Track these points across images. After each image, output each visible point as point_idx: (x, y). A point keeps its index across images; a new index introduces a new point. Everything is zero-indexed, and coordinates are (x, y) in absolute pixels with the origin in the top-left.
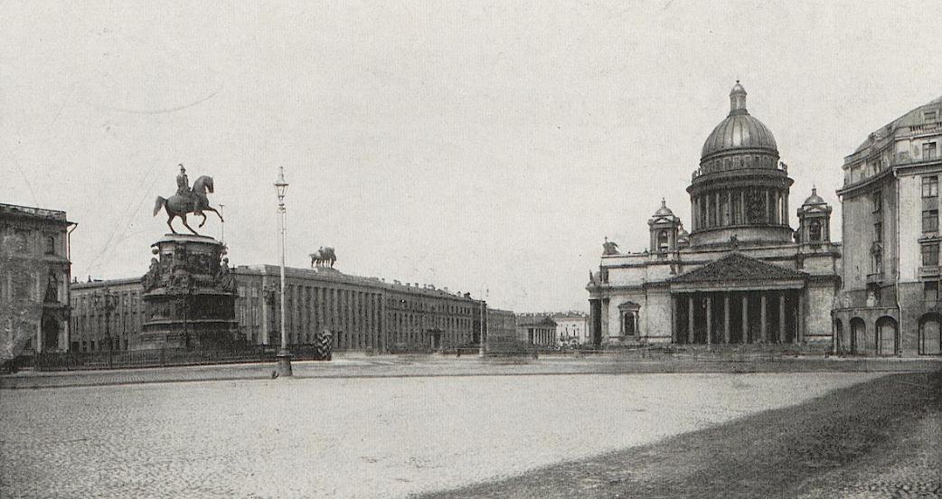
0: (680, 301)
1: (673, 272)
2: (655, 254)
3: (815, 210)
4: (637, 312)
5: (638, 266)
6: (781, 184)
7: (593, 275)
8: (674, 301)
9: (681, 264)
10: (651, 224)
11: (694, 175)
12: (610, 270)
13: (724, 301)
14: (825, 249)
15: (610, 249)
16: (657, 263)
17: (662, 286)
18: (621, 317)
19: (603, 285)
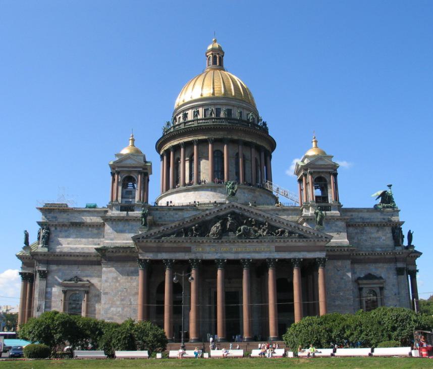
0: (153, 270)
3: (320, 163)
4: (87, 292)
10: (113, 167)
12: (53, 229)
14: (336, 213)
19: (41, 249)
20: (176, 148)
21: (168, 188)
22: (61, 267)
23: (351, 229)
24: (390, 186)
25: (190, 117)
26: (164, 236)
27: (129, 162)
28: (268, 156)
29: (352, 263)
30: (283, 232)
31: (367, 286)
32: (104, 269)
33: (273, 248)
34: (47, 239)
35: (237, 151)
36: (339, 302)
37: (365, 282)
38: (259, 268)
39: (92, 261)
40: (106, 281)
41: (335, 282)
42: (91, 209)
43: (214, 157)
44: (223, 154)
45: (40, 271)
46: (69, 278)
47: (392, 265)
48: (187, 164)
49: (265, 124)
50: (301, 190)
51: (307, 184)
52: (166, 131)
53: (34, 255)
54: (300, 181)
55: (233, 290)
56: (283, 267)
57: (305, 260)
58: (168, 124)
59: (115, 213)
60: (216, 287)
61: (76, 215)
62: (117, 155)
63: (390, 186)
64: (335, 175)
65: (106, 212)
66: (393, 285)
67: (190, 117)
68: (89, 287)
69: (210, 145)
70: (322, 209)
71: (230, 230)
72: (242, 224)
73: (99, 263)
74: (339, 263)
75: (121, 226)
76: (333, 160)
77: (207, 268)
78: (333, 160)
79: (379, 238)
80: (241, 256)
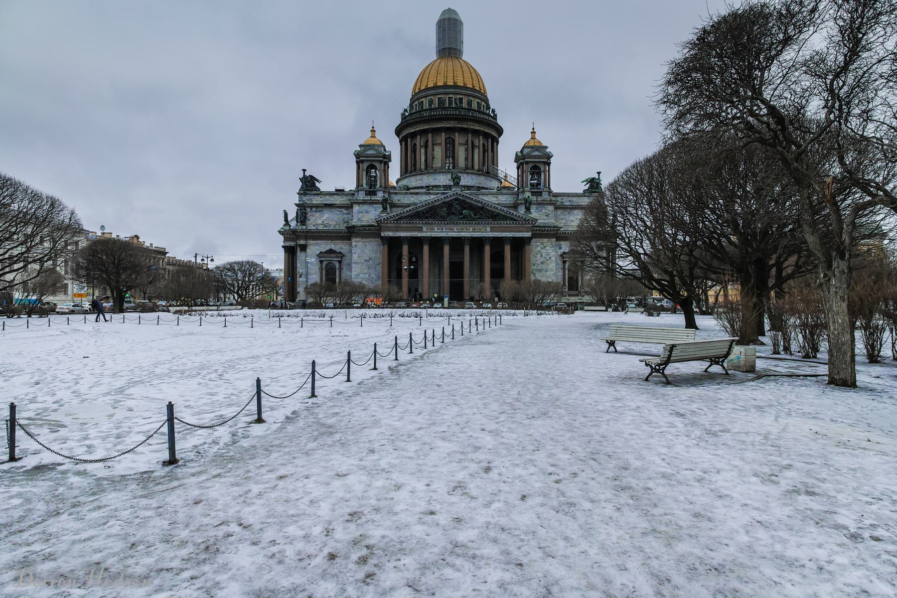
0: (393, 245)
1: (385, 209)
2: (361, 190)
3: (536, 153)
4: (340, 262)
5: (340, 207)
6: (490, 131)
7: (289, 219)
8: (386, 247)
9: (393, 206)
10: (357, 155)
11: (403, 115)
13: (442, 250)
15: (309, 184)
16: (364, 202)
17: (370, 232)
18: (321, 269)
20: (413, 135)
21: (406, 173)
23: (559, 212)
24: (599, 173)
25: (426, 106)
26: (401, 218)
27: (371, 152)
28: (495, 141)
29: (557, 240)
30: (497, 215)
32: (354, 244)
33: (488, 229)
34: (302, 217)
38: (477, 244)
42: (340, 192)
43: (446, 144)
44: (454, 141)
48: (423, 150)
49: (493, 111)
50: (518, 176)
51: (523, 172)
52: (404, 117)
53: (294, 232)
54: (518, 168)
55: (458, 260)
56: (497, 243)
57: (514, 238)
58: (406, 110)
59: (361, 196)
60: (443, 258)
61: (328, 197)
62: (360, 146)
63: (599, 173)
64: (549, 164)
65: (353, 194)
67: (426, 106)
69: (443, 134)
70: (533, 193)
71: (454, 214)
72: (465, 209)
73: (349, 238)
74: (545, 240)
75: (365, 207)
76: (548, 150)
77: (436, 244)
78: (548, 150)
80: (463, 234)
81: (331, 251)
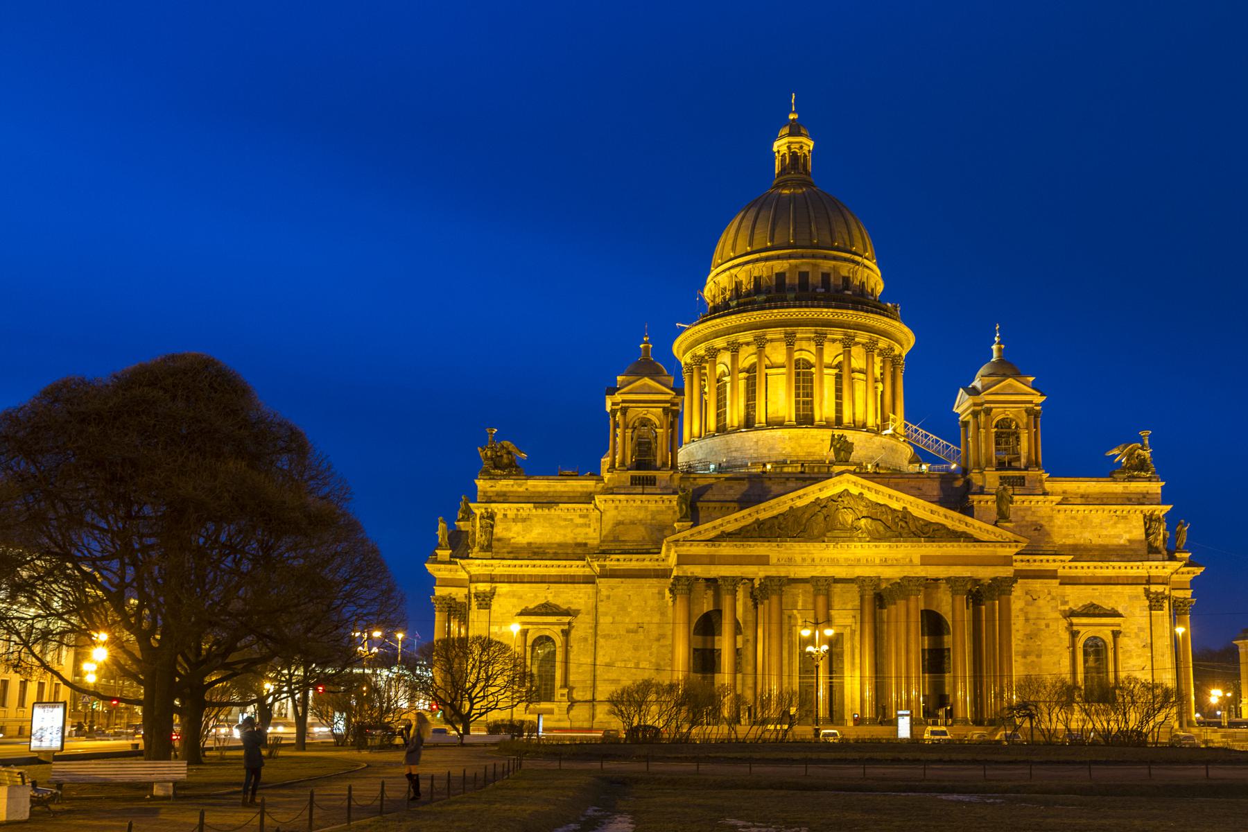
4: (566, 633)
22: (516, 587)
31: (1089, 628)
32: (604, 592)
33: (917, 560)
35: (841, 358)
36: (1035, 659)
37: (1084, 620)
39: (573, 576)
40: (606, 614)
41: (1027, 620)
45: (476, 596)
46: (531, 606)
47: (1140, 589)
66: (1141, 629)
68: (569, 623)
79: (1120, 536)
81: (547, 609)
